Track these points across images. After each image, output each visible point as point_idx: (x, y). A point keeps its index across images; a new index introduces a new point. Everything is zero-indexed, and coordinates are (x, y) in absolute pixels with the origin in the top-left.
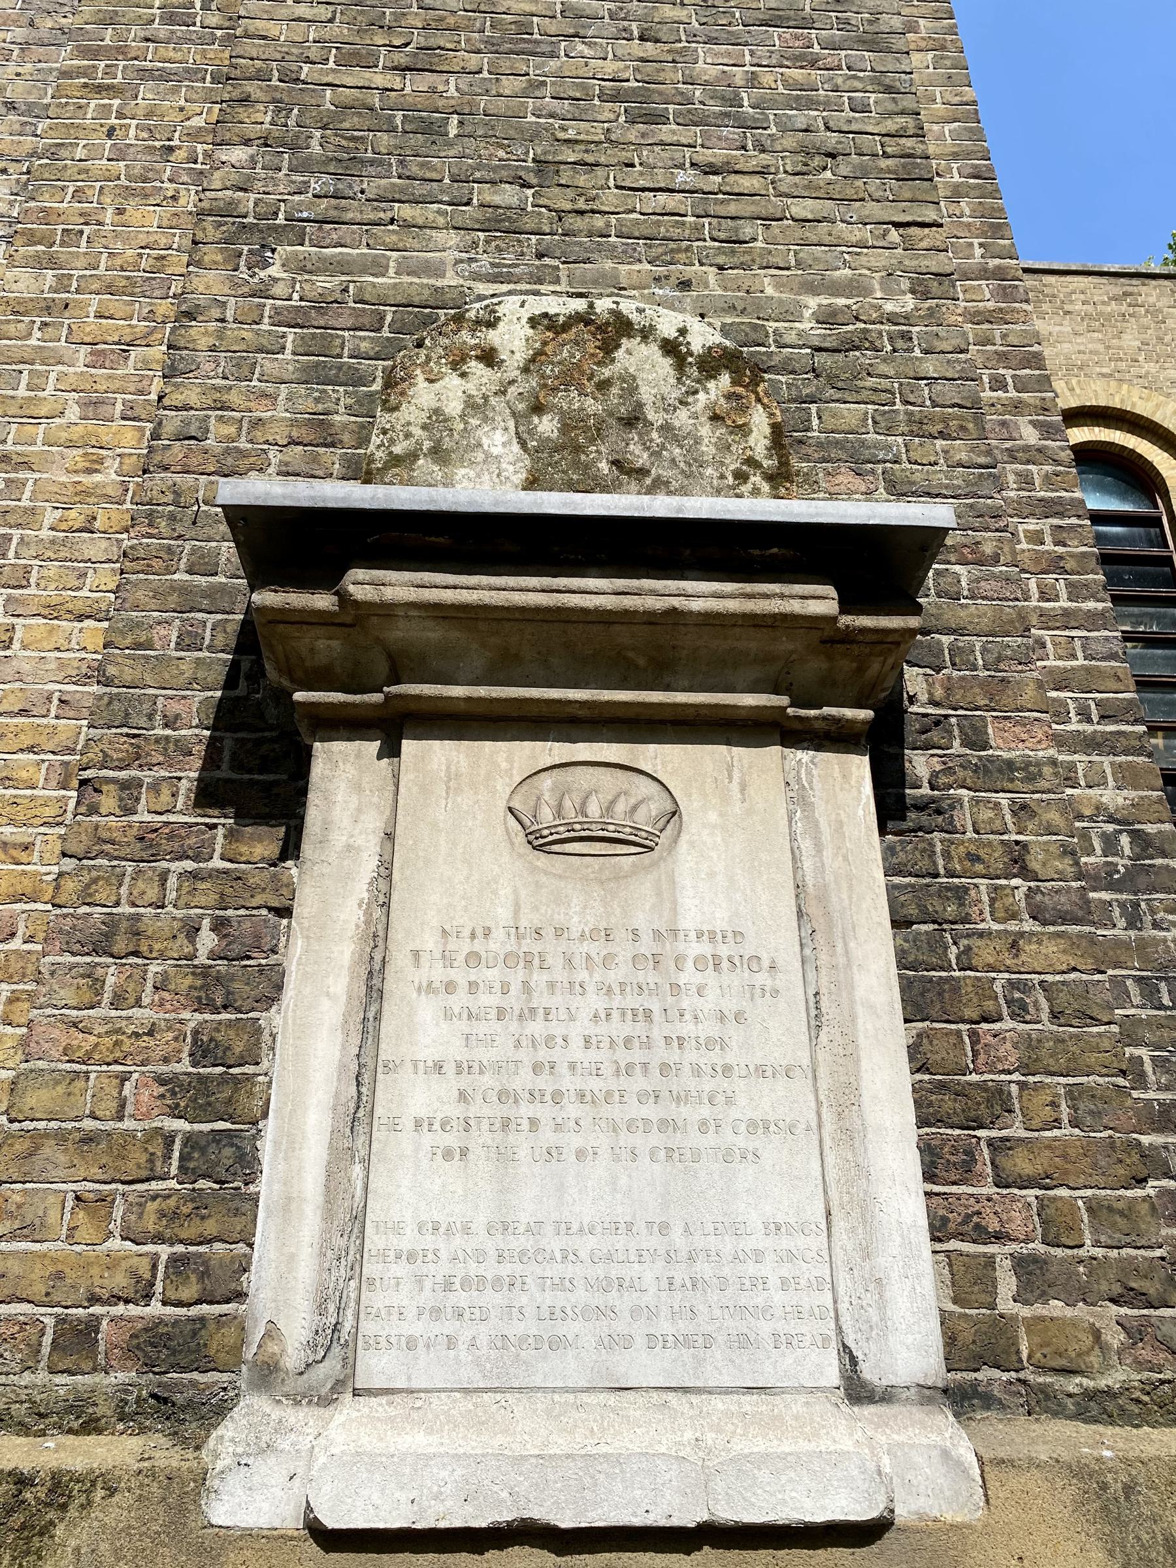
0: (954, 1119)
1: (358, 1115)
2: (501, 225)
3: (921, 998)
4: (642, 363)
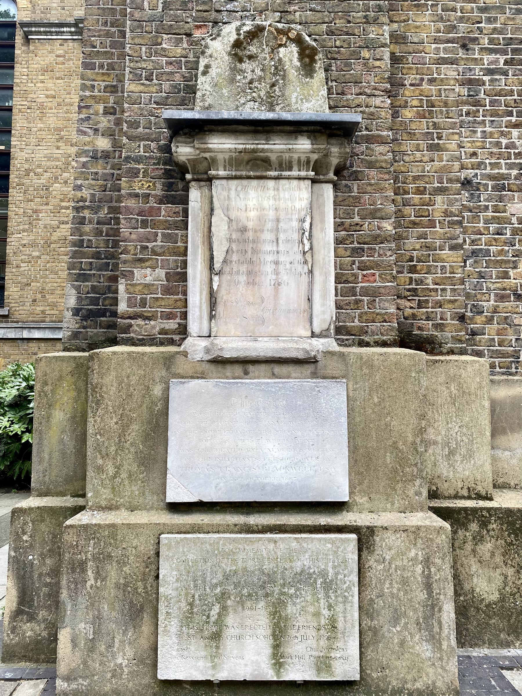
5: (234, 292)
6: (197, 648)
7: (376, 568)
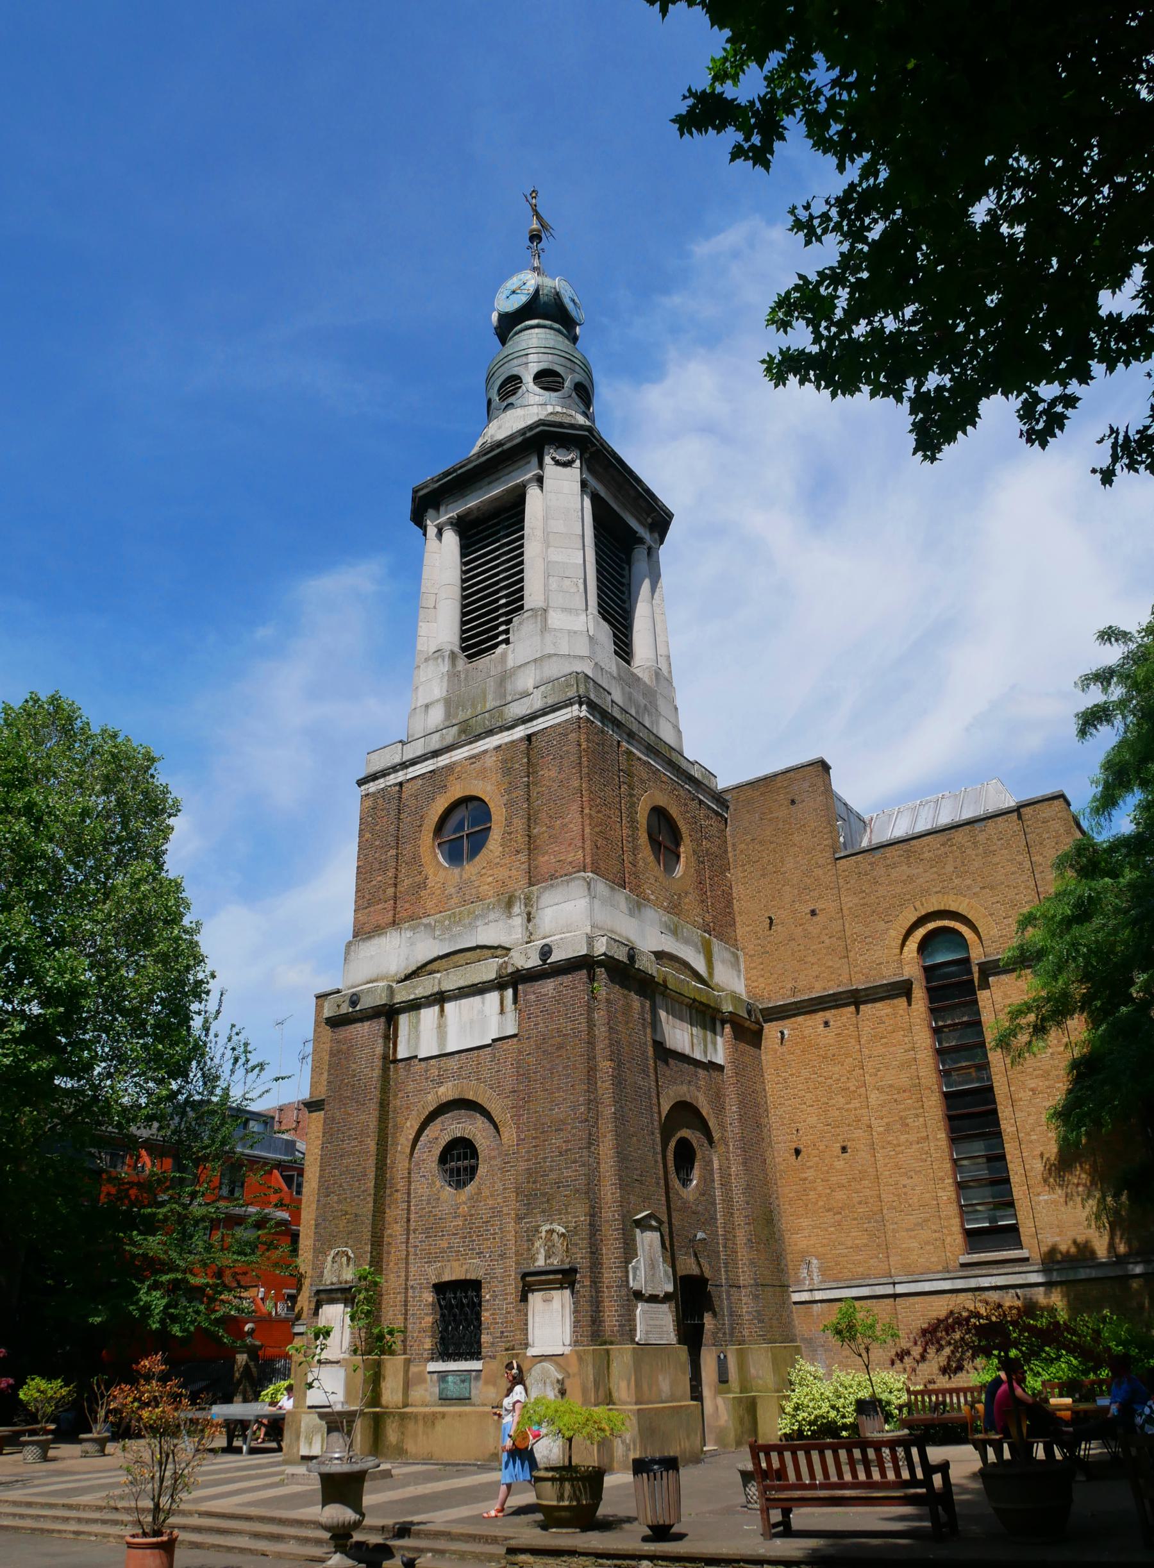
0: (576, 1324)
4: (555, 1236)
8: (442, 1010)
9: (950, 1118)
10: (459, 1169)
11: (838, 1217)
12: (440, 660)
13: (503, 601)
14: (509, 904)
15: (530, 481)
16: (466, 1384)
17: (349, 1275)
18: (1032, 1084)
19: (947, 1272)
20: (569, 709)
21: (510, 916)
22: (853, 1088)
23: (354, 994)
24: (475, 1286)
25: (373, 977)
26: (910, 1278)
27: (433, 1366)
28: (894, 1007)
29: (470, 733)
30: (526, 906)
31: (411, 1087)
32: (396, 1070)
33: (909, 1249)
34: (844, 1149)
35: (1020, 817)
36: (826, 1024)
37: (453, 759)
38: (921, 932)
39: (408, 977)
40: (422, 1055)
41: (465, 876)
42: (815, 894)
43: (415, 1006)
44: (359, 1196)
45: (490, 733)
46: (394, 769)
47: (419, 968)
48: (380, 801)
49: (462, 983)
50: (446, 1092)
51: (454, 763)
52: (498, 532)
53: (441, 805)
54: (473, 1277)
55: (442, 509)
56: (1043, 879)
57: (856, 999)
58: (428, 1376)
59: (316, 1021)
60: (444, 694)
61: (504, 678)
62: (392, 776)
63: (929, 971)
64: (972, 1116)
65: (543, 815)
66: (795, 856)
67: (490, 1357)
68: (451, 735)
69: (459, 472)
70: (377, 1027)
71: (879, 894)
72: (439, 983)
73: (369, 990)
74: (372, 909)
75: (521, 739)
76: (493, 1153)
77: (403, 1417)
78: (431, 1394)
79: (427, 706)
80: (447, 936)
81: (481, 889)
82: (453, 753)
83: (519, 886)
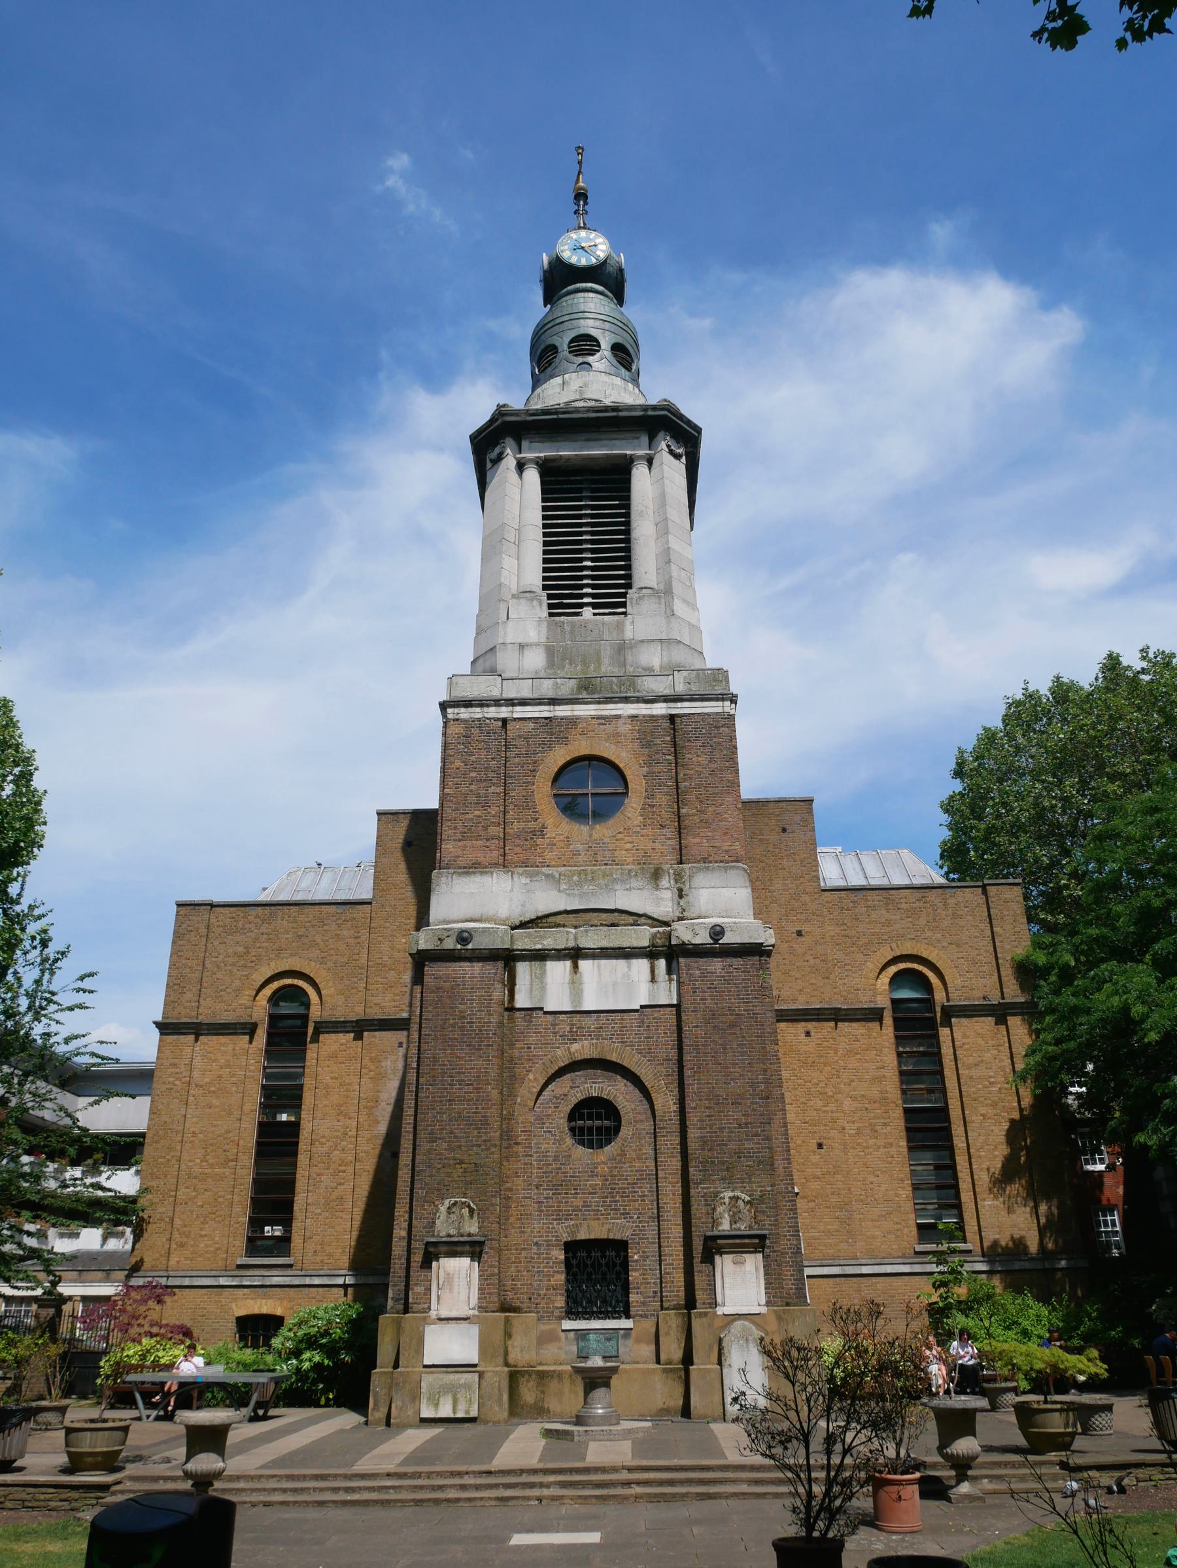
1: (723, 1287)
2: (723, 1179)
3: (765, 1274)
4: (740, 1202)
5: (445, 1295)
6: (432, 1408)
7: (483, 1382)
8: (575, 966)
9: (908, 1130)
10: (590, 1129)
11: (812, 1204)
12: (535, 603)
13: (589, 564)
14: (656, 875)
15: (640, 457)
16: (613, 1343)
17: (472, 1227)
18: (983, 1110)
19: (904, 1259)
20: (720, 703)
21: (657, 888)
22: (830, 1094)
23: (462, 931)
24: (621, 1246)
25: (475, 916)
26: (874, 1261)
27: (567, 1324)
28: (869, 1029)
29: (588, 690)
30: (676, 882)
31: (533, 1038)
32: (511, 1018)
33: (873, 1237)
34: (820, 1146)
35: (985, 892)
36: (808, 1034)
37: (576, 713)
38: (893, 970)
39: (523, 925)
40: (549, 1008)
41: (596, 836)
42: (803, 917)
43: (540, 956)
44: (480, 1146)
45: (626, 700)
46: (497, 702)
47: (538, 918)
48: (476, 731)
49: (605, 943)
50: (582, 1049)
51: (578, 718)
52: (580, 491)
53: (559, 756)
54: (618, 1237)
55: (525, 444)
56: (1002, 947)
57: (837, 1016)
58: (563, 1334)
59: (175, 932)
60: (544, 640)
61: (622, 648)
62: (492, 709)
63: (894, 1002)
64: (929, 1130)
65: (692, 798)
66: (784, 879)
67: (641, 1316)
68: (567, 688)
69: (561, 416)
70: (495, 970)
71: (859, 929)
72: (576, 939)
73: (484, 930)
74: (468, 843)
75: (663, 717)
76: (639, 1117)
77: (542, 1375)
78: (567, 1353)
79: (522, 647)
80: (576, 892)
81: (617, 853)
82: (576, 707)
83: (668, 861)
